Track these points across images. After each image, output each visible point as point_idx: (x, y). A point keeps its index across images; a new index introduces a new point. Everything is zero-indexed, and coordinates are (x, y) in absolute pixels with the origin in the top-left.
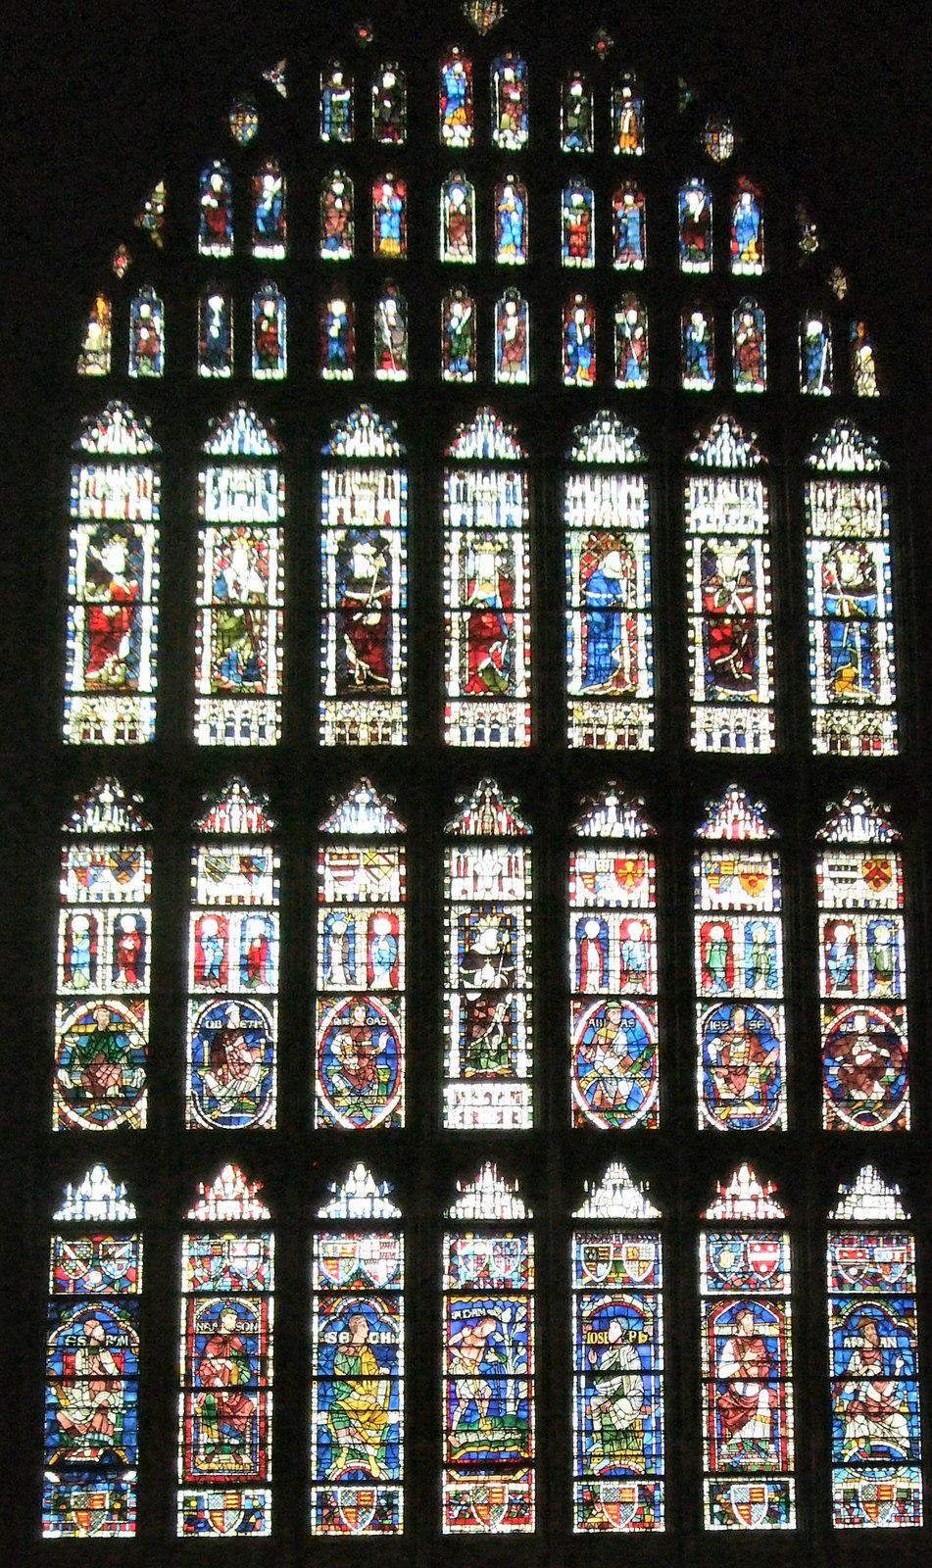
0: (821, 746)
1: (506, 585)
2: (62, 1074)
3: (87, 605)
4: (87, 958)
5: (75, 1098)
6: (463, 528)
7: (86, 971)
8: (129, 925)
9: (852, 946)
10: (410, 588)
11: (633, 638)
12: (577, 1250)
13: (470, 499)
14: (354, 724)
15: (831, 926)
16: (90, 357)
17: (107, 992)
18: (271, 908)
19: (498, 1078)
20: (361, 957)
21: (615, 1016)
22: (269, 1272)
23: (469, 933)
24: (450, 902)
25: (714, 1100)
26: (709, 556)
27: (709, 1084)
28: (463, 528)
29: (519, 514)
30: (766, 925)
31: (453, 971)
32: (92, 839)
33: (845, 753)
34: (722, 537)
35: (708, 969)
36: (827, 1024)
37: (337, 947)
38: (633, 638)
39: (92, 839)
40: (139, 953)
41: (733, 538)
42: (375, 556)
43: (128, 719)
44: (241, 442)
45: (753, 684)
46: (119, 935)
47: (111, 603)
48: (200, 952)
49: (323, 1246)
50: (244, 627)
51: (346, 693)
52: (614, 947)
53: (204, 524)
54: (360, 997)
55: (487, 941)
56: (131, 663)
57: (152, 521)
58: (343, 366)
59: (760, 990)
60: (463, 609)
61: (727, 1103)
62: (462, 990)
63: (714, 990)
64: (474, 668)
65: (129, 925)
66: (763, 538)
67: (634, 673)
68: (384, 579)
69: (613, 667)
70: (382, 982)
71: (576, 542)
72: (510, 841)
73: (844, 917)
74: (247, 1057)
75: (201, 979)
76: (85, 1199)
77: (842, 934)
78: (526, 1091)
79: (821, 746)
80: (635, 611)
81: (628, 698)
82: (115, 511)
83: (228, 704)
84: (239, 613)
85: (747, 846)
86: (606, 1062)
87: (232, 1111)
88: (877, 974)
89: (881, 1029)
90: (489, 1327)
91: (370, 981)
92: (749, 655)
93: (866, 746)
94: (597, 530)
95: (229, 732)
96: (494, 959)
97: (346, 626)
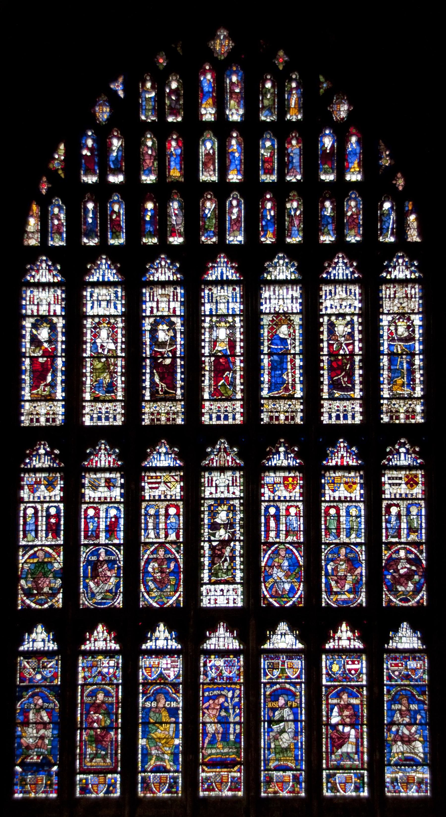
2: (23, 582)
5: (28, 594)
7: (33, 533)
8: (53, 511)
9: (399, 516)
12: (264, 663)
15: (389, 507)
17: (43, 543)
18: (119, 503)
19: (226, 582)
20: (162, 526)
21: (282, 553)
22: (119, 673)
23: (213, 514)
25: (330, 591)
31: (206, 531)
35: (327, 529)
37: (151, 521)
40: (58, 524)
46: (48, 516)
48: (86, 524)
49: (145, 662)
52: (283, 520)
55: (222, 517)
59: (353, 538)
61: (337, 593)
62: (210, 541)
65: (53, 511)
73: (395, 502)
74: (109, 574)
75: (86, 537)
76: (34, 641)
77: (394, 510)
78: (240, 589)
86: (278, 574)
87: (102, 599)
88: (411, 530)
89: (412, 556)
90: (222, 700)
91: (167, 536)
96: (225, 526)
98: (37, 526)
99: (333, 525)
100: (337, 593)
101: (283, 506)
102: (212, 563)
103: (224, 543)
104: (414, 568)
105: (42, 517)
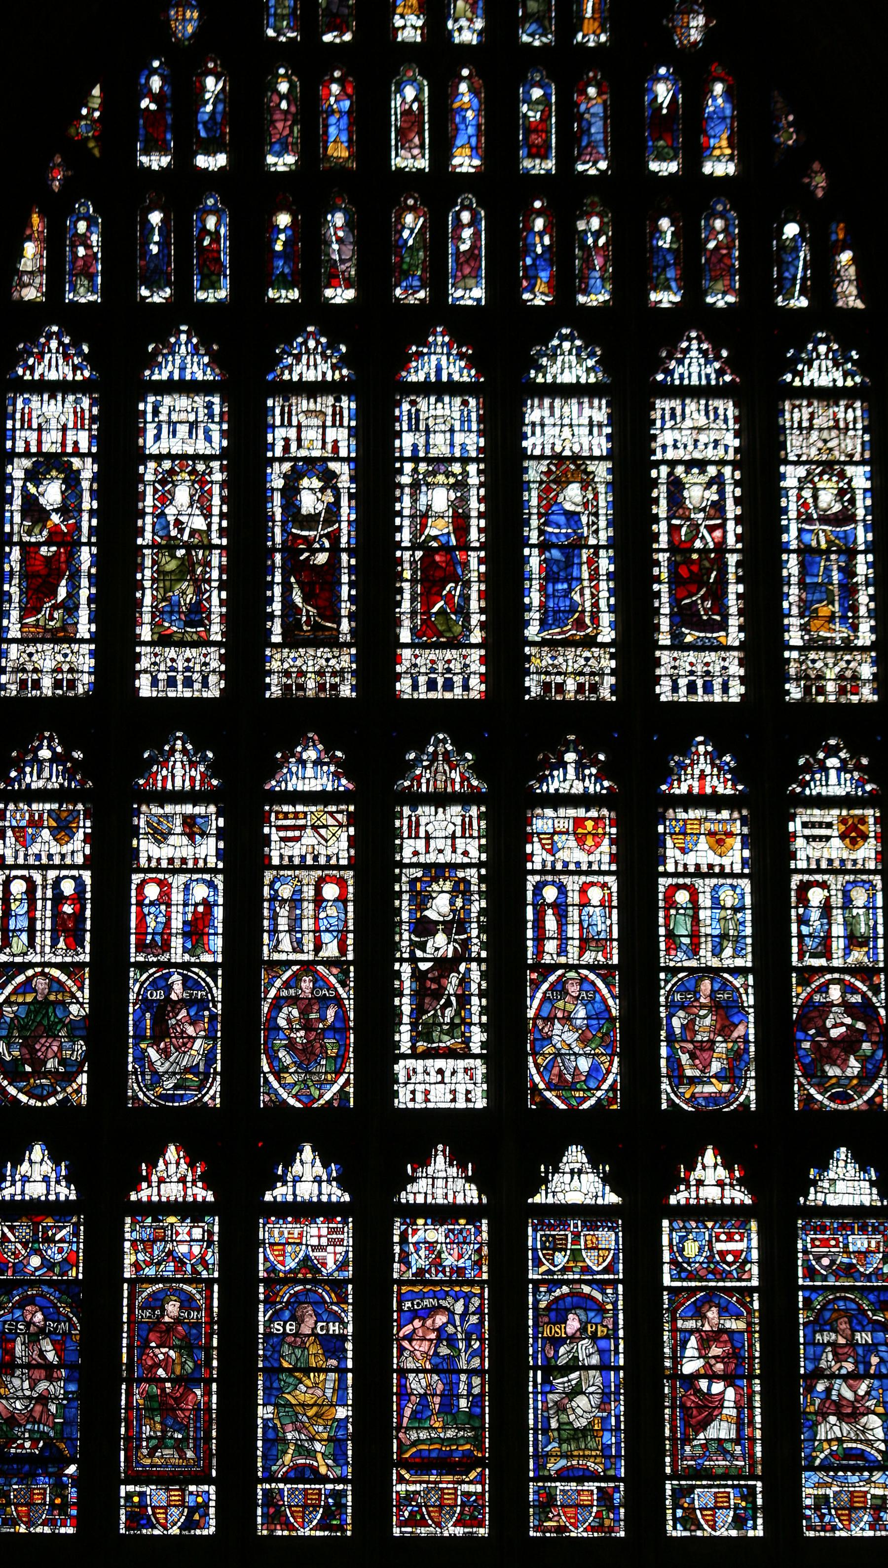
0: (795, 692)
1: (461, 523)
3: (21, 544)
4: (24, 923)
6: (415, 459)
8: (68, 887)
9: (826, 909)
10: (358, 525)
11: (595, 576)
13: (422, 427)
14: (302, 673)
15: (804, 887)
16: (25, 279)
18: (214, 871)
19: (450, 1054)
20: (307, 924)
21: (573, 989)
23: (421, 900)
24: (402, 865)
25: (678, 1077)
26: (676, 487)
27: (673, 1061)
28: (415, 459)
29: (472, 442)
30: (733, 887)
32: (31, 796)
33: (821, 699)
34: (690, 464)
36: (799, 994)
38: (595, 576)
39: (31, 796)
40: (79, 917)
41: (702, 464)
42: (322, 490)
43: (66, 667)
44: (182, 369)
45: (723, 626)
46: (59, 898)
47: (48, 543)
48: (142, 918)
50: (187, 568)
51: (292, 640)
52: (573, 914)
53: (145, 458)
54: (307, 967)
56: (70, 607)
57: (89, 454)
58: (288, 287)
60: (413, 548)
61: (692, 1081)
63: (681, 959)
64: (427, 612)
66: (735, 465)
67: (595, 618)
68: (333, 510)
69: (573, 608)
70: (331, 950)
71: (534, 472)
72: (464, 799)
73: (819, 877)
77: (816, 896)
78: (480, 1068)
79: (795, 692)
80: (597, 547)
81: (590, 642)
82: (51, 443)
83: (171, 652)
84: (180, 553)
85: (715, 802)
88: (853, 940)
89: (856, 999)
91: (318, 947)
92: (718, 593)
93: (842, 691)
94: (558, 458)
95: (171, 682)
97: (293, 566)
98: (32, 921)
99: (683, 928)
100: (692, 1081)
101: (573, 883)
102: (418, 1010)
103: (445, 966)
104: (860, 1025)
105: (44, 899)
